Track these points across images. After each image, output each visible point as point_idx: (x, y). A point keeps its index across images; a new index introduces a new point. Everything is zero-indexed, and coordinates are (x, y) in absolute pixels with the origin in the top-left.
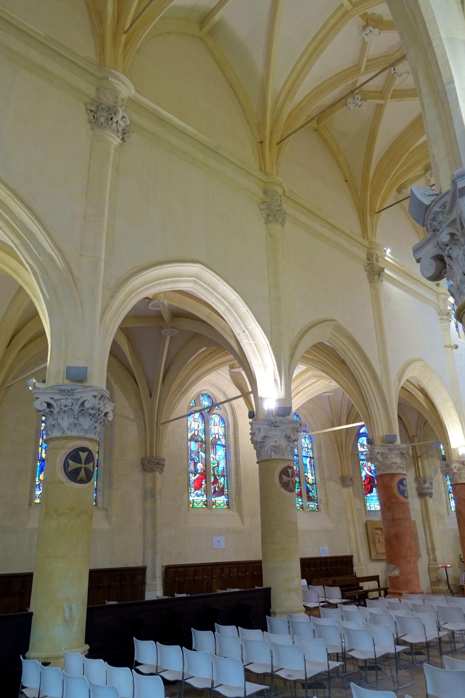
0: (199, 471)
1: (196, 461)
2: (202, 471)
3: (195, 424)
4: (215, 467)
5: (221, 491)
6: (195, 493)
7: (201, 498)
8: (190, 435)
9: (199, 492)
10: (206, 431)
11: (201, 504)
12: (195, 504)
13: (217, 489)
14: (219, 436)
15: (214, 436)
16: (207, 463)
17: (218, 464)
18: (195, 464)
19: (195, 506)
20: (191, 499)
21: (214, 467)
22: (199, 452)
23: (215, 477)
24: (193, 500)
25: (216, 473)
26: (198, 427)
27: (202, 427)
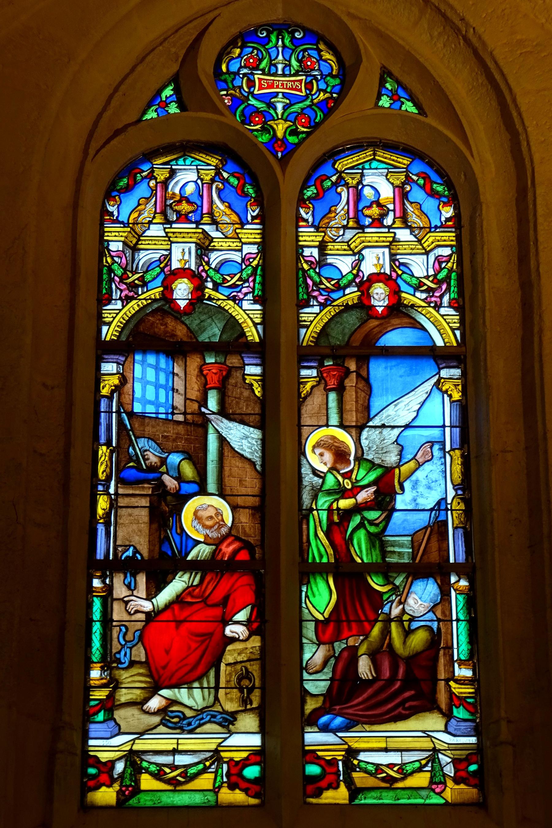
0: (201, 552)
1: (170, 482)
2: (228, 549)
3: (178, 232)
4: (358, 509)
5: (409, 682)
6: (155, 703)
7: (203, 741)
8: (116, 316)
9: (192, 698)
10: (279, 276)
11: (205, 781)
12: (147, 782)
13: (364, 667)
14: (395, 292)
15: (352, 294)
16: (274, 487)
17: (386, 488)
18: (165, 508)
19: (145, 800)
20: (106, 746)
21: (347, 514)
22: (201, 424)
23: (347, 575)
24: (133, 758)
25: (361, 550)
26: (204, 248)
27: (237, 246)
